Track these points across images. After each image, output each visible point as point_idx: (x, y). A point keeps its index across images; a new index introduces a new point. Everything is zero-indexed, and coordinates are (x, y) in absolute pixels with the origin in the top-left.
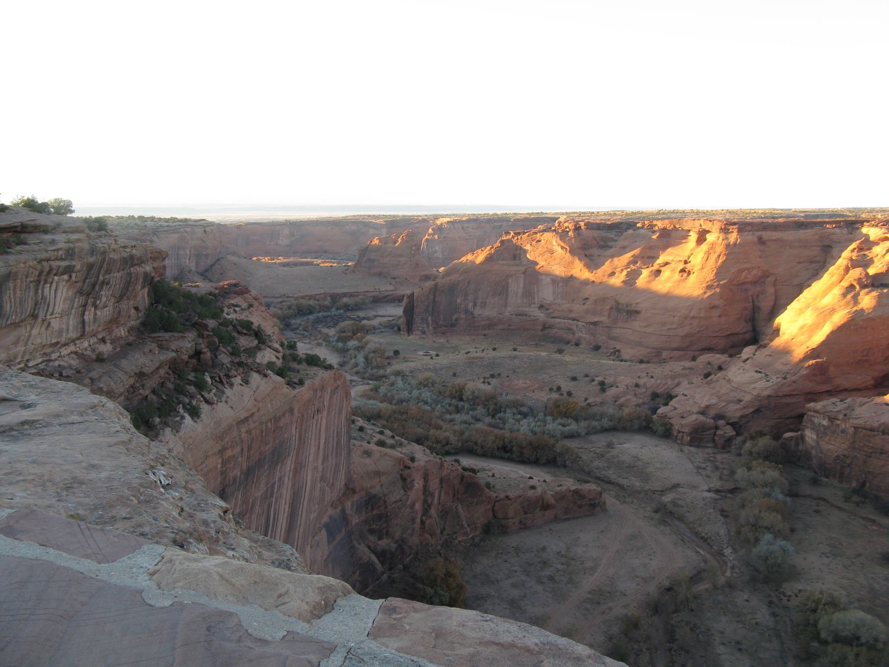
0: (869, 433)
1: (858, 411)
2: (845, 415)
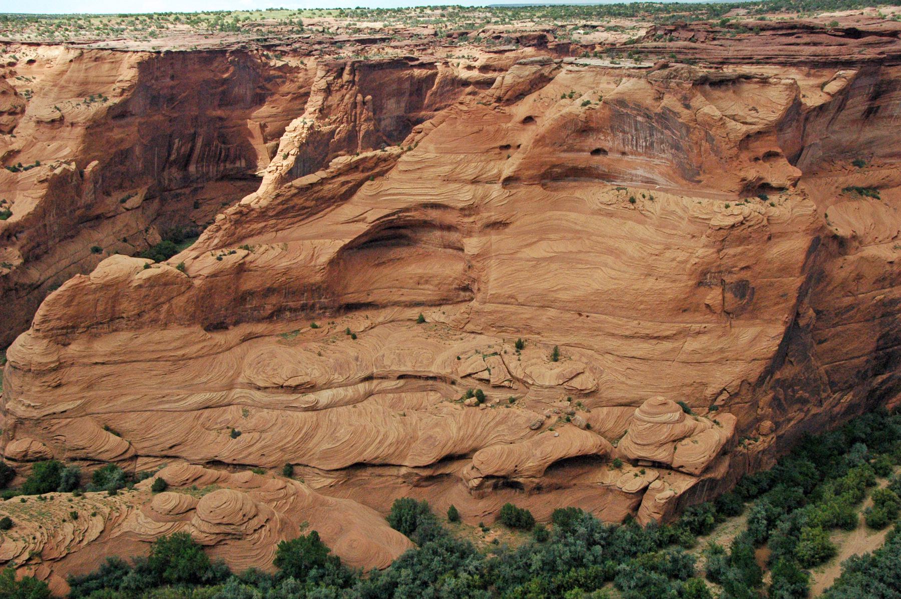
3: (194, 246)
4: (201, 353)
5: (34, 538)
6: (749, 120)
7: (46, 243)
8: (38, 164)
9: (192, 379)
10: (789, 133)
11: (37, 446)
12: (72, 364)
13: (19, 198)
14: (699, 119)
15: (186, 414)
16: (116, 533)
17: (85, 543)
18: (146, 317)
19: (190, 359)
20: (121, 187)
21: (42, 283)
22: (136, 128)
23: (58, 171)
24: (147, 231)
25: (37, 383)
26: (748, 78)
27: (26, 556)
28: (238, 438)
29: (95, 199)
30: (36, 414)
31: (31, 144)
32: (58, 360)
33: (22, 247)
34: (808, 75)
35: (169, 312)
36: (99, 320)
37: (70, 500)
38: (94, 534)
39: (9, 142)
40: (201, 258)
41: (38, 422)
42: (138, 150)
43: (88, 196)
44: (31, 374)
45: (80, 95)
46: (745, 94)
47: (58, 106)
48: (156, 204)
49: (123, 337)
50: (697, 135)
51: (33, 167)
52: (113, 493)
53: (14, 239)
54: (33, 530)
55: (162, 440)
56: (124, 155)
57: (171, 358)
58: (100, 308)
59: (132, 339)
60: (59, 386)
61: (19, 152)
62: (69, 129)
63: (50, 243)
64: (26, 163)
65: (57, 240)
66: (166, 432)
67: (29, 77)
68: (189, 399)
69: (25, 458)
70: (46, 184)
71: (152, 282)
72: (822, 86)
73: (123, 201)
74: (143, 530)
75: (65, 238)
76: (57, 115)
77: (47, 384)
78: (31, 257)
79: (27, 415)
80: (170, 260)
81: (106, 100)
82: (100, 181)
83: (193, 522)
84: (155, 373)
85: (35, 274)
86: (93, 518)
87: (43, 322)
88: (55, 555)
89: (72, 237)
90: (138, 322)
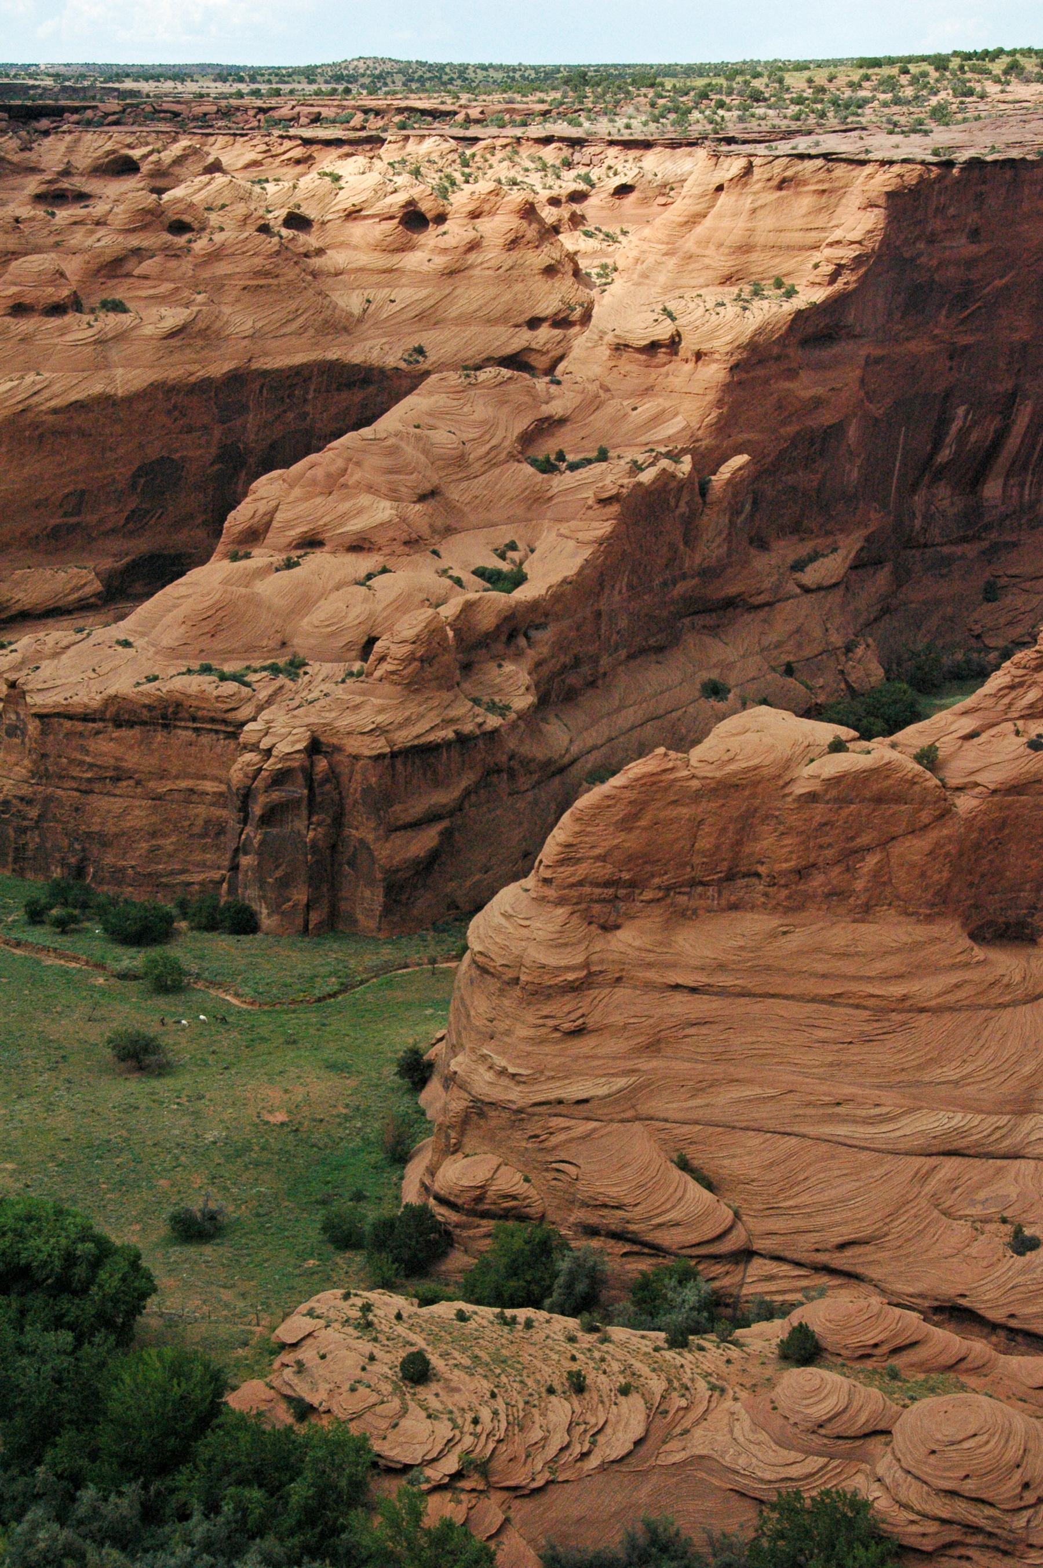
0: (80, 726)
1: (47, 668)
2: (12, 685)
3: (970, 701)
4: (951, 998)
5: (476, 1421)
7: (595, 660)
8: (603, 456)
9: (920, 1067)
11: (510, 1181)
12: (619, 979)
13: (547, 538)
15: (890, 1163)
16: (674, 1453)
17: (593, 1462)
18: (817, 882)
19: (922, 1010)
20: (796, 529)
21: (573, 762)
22: (858, 372)
23: (647, 477)
24: (849, 649)
25: (530, 1018)
27: (451, 1464)
28: (1030, 1256)
29: (729, 555)
30: (516, 1095)
31: (593, 404)
32: (586, 965)
33: (539, 664)
35: (880, 878)
36: (698, 874)
37: (572, 1339)
38: (617, 1443)
39: (543, 395)
40: (984, 737)
41: (520, 1115)
42: (852, 432)
43: (710, 548)
44: (517, 992)
45: (727, 280)
47: (671, 306)
48: (883, 577)
49: (755, 924)
51: (589, 462)
52: (678, 1341)
53: (522, 642)
54: (475, 1402)
55: (820, 1220)
56: (821, 442)
57: (871, 1002)
58: (704, 843)
59: (773, 935)
60: (579, 1032)
61: (562, 421)
62: (691, 365)
63: (605, 661)
64: (576, 451)
65: (623, 653)
66: (837, 1199)
67: (614, 229)
68: (904, 1121)
69: (477, 1205)
70: (614, 509)
71: (845, 789)
73: (799, 566)
74: (742, 1461)
75: (643, 651)
76: (663, 331)
77: (551, 1022)
78: (555, 694)
79: (496, 1094)
80: (899, 736)
81: (791, 293)
82: (748, 507)
83: (880, 1471)
84: (822, 1034)
85: (559, 737)
86: (621, 1399)
87: (561, 862)
88: (519, 1477)
89: (660, 649)
90: (794, 891)
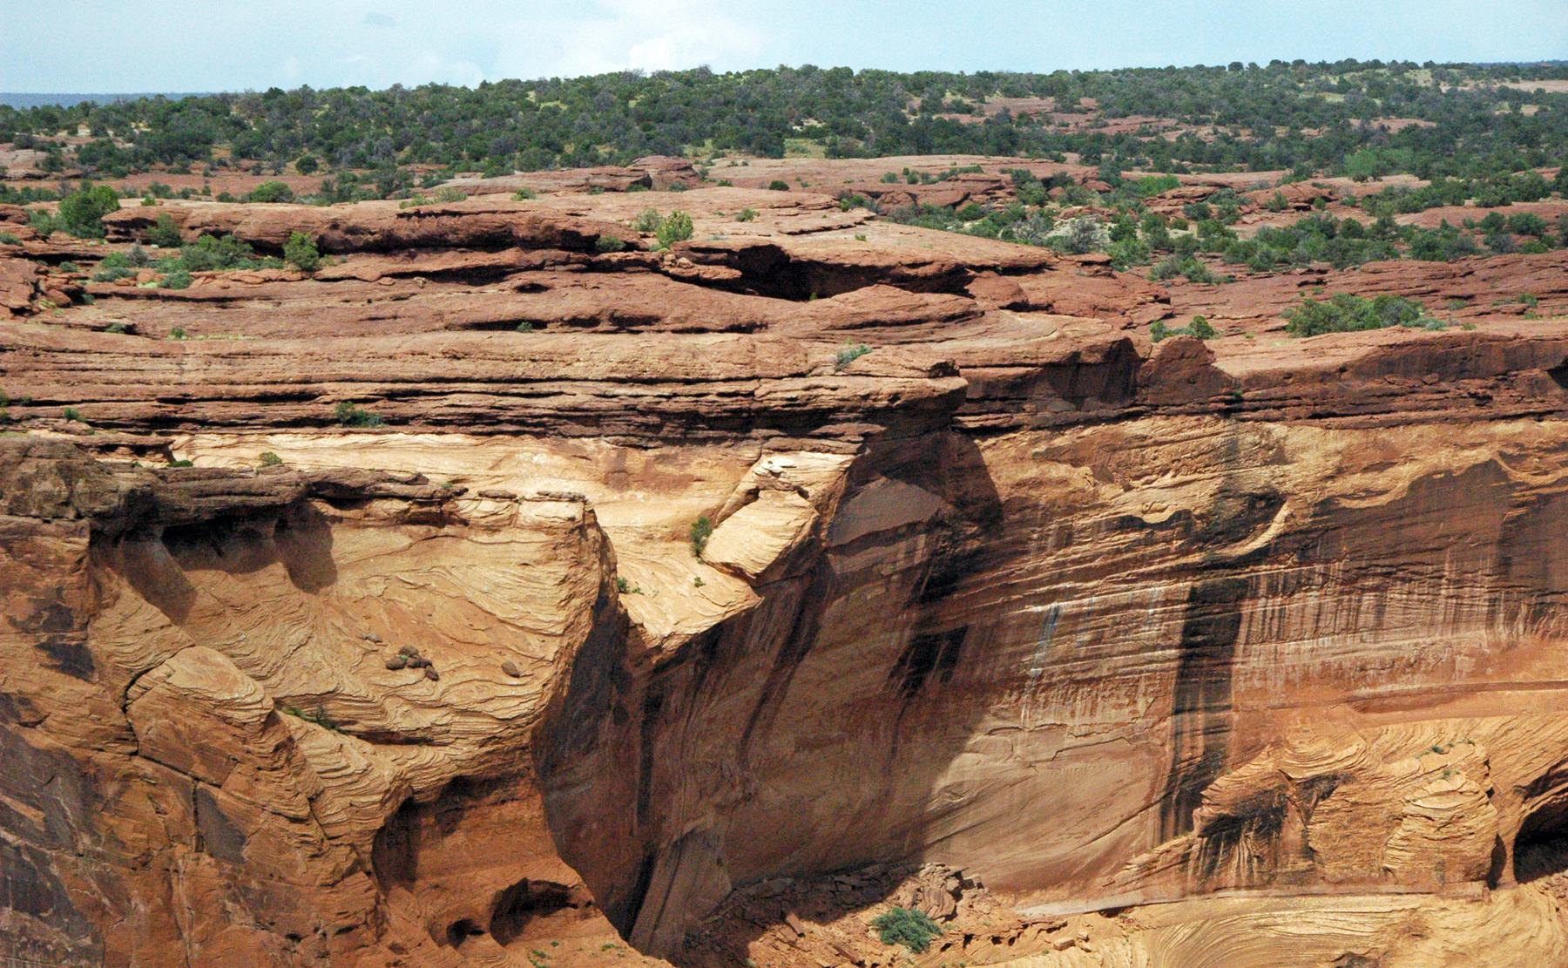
6: (400, 719)
10: (592, 783)
14: (149, 728)
26: (348, 495)
34: (618, 478)
46: (346, 584)
50: (150, 812)
72: (698, 532)
